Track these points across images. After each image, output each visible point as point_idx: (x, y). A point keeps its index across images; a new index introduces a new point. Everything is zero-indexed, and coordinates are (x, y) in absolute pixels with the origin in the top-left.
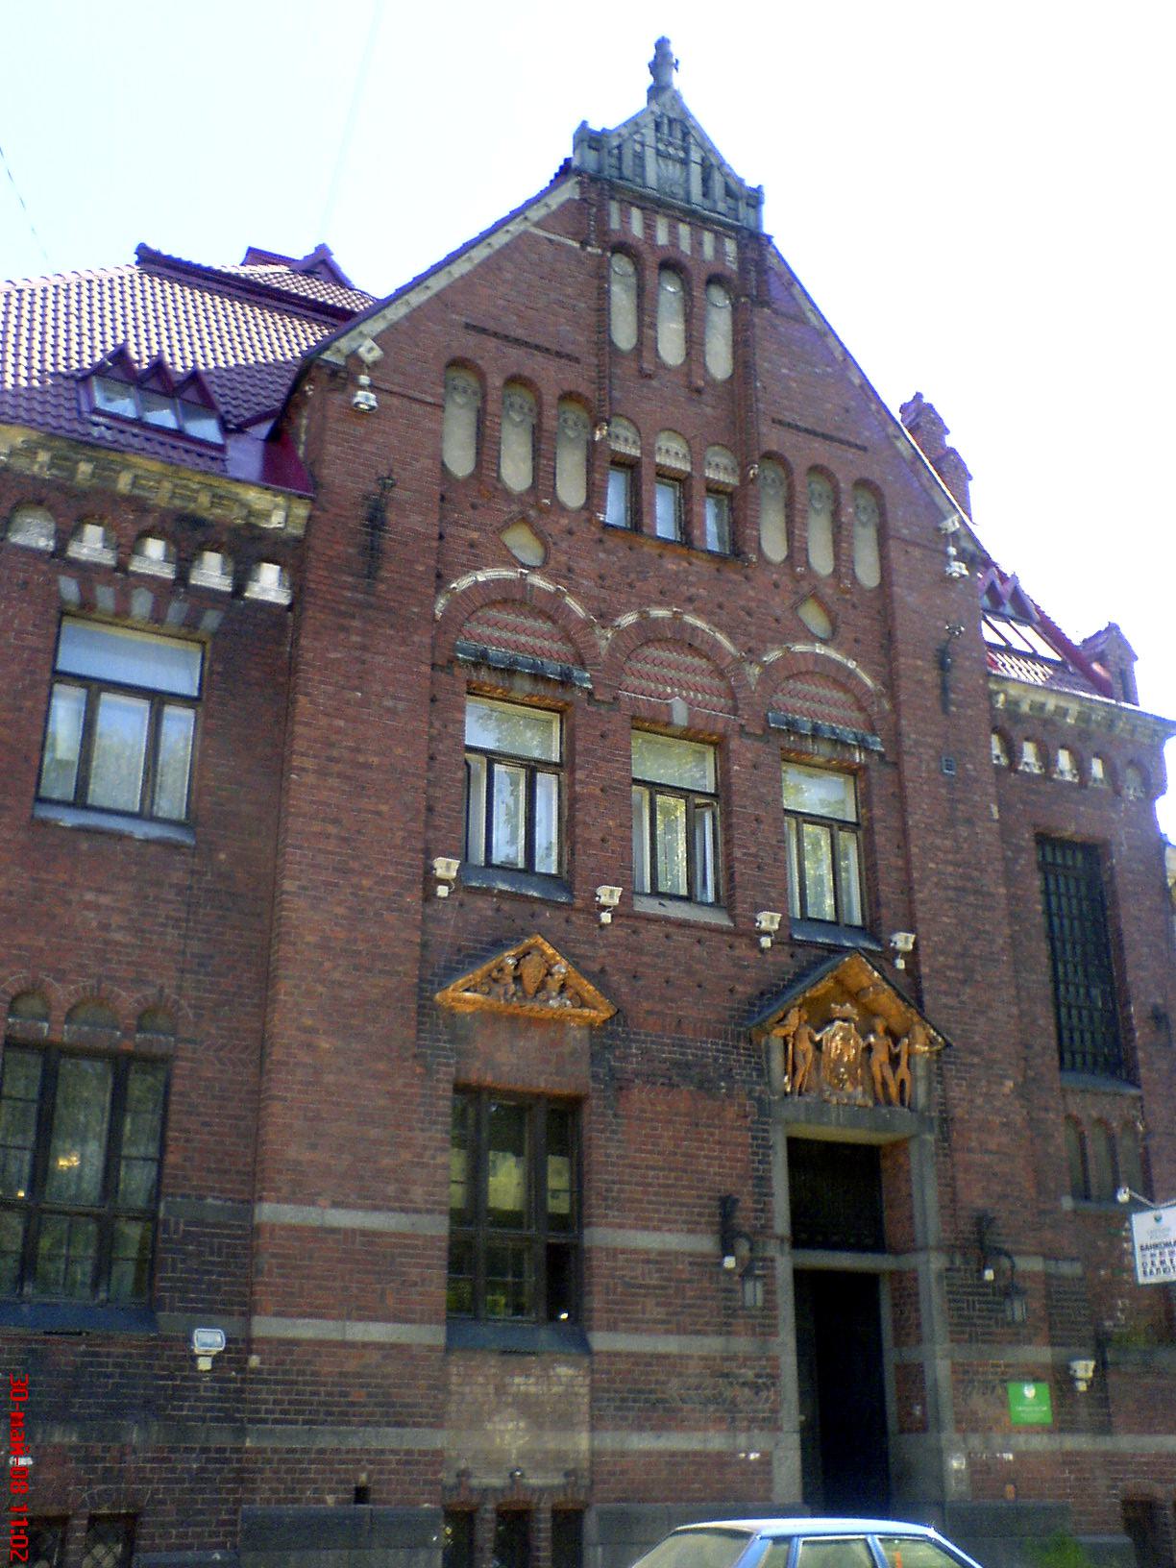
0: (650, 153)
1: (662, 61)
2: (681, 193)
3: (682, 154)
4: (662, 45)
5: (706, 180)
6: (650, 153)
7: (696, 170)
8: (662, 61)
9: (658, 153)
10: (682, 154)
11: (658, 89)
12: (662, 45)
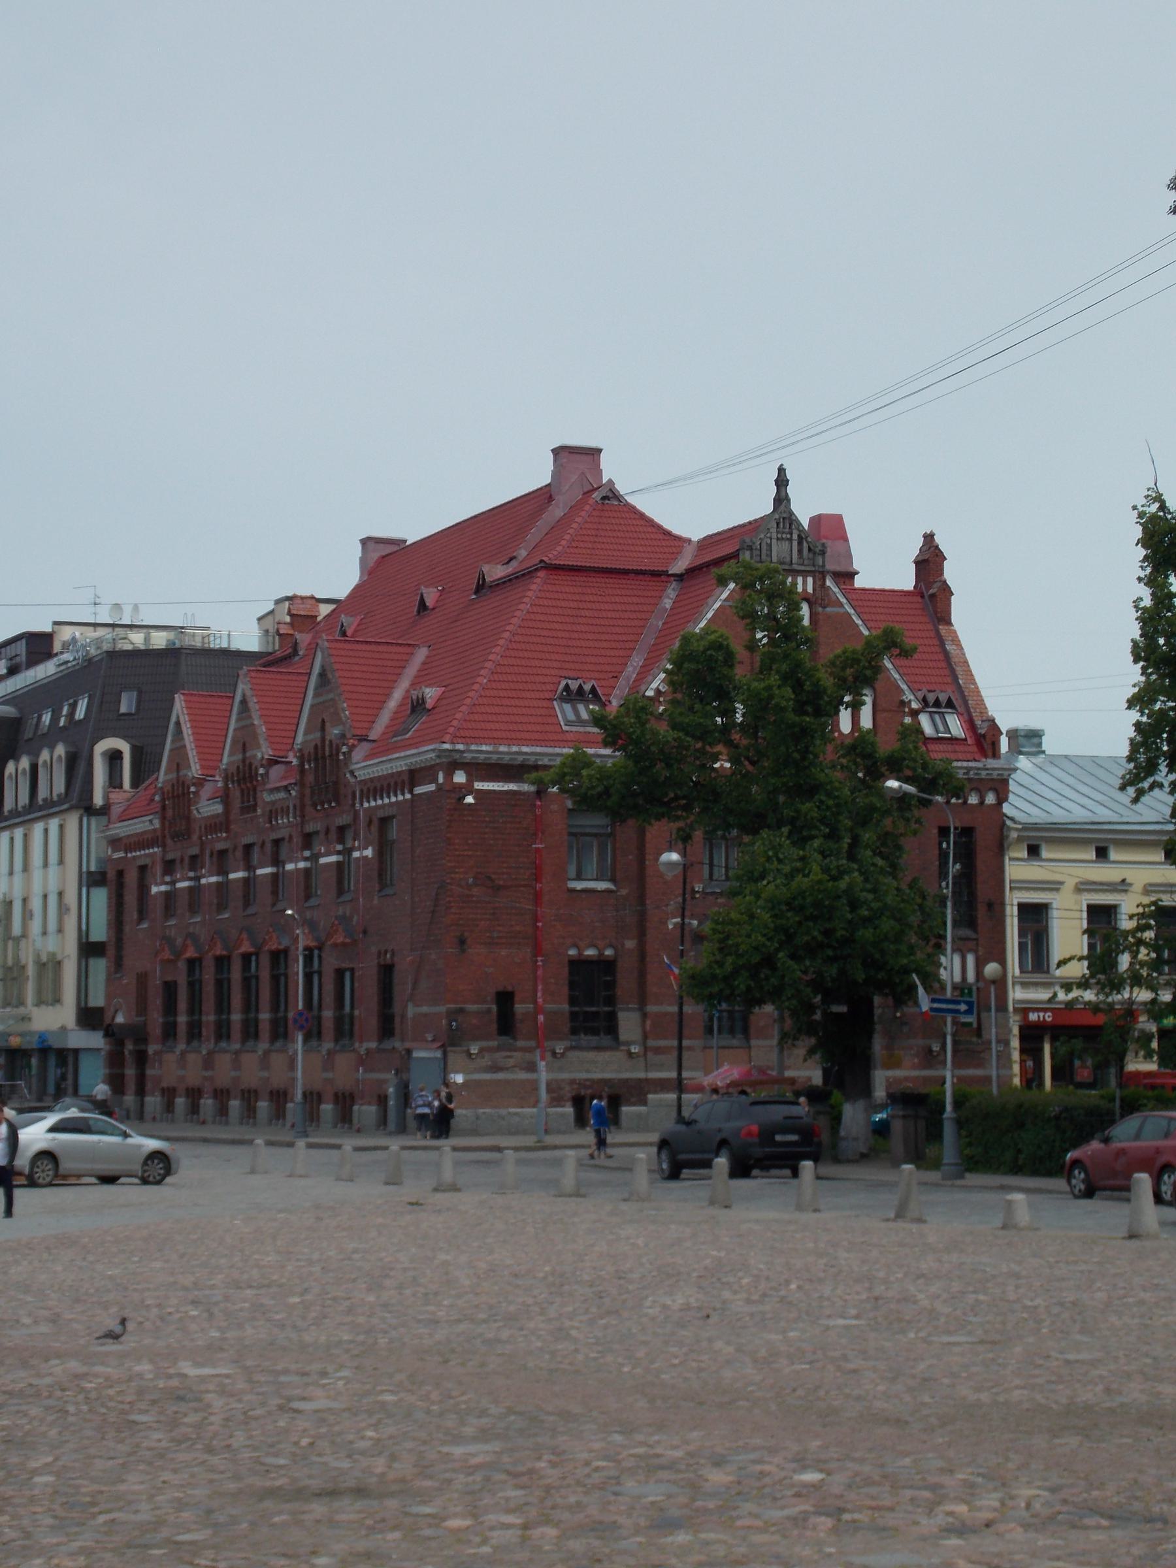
0: (774, 541)
1: (782, 481)
2: (788, 560)
3: (789, 536)
4: (781, 470)
5: (800, 543)
6: (774, 541)
7: (795, 543)
8: (782, 481)
9: (778, 539)
10: (789, 536)
11: (781, 500)
12: (781, 470)
